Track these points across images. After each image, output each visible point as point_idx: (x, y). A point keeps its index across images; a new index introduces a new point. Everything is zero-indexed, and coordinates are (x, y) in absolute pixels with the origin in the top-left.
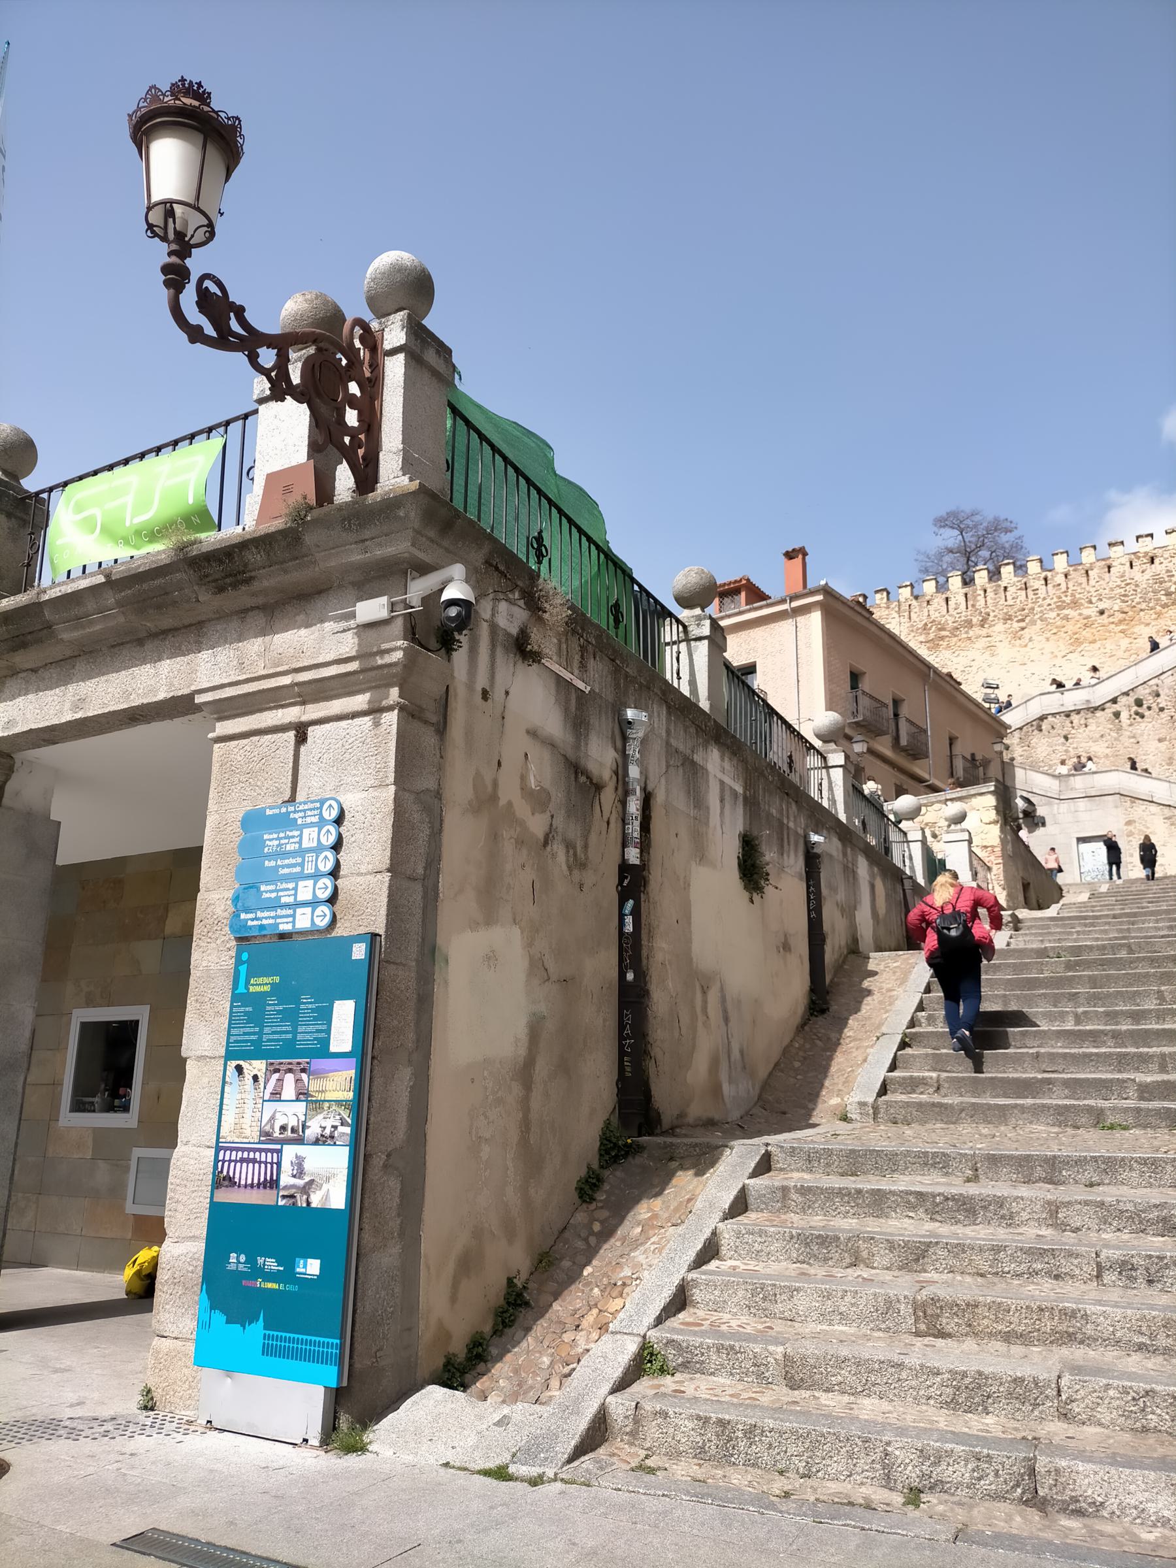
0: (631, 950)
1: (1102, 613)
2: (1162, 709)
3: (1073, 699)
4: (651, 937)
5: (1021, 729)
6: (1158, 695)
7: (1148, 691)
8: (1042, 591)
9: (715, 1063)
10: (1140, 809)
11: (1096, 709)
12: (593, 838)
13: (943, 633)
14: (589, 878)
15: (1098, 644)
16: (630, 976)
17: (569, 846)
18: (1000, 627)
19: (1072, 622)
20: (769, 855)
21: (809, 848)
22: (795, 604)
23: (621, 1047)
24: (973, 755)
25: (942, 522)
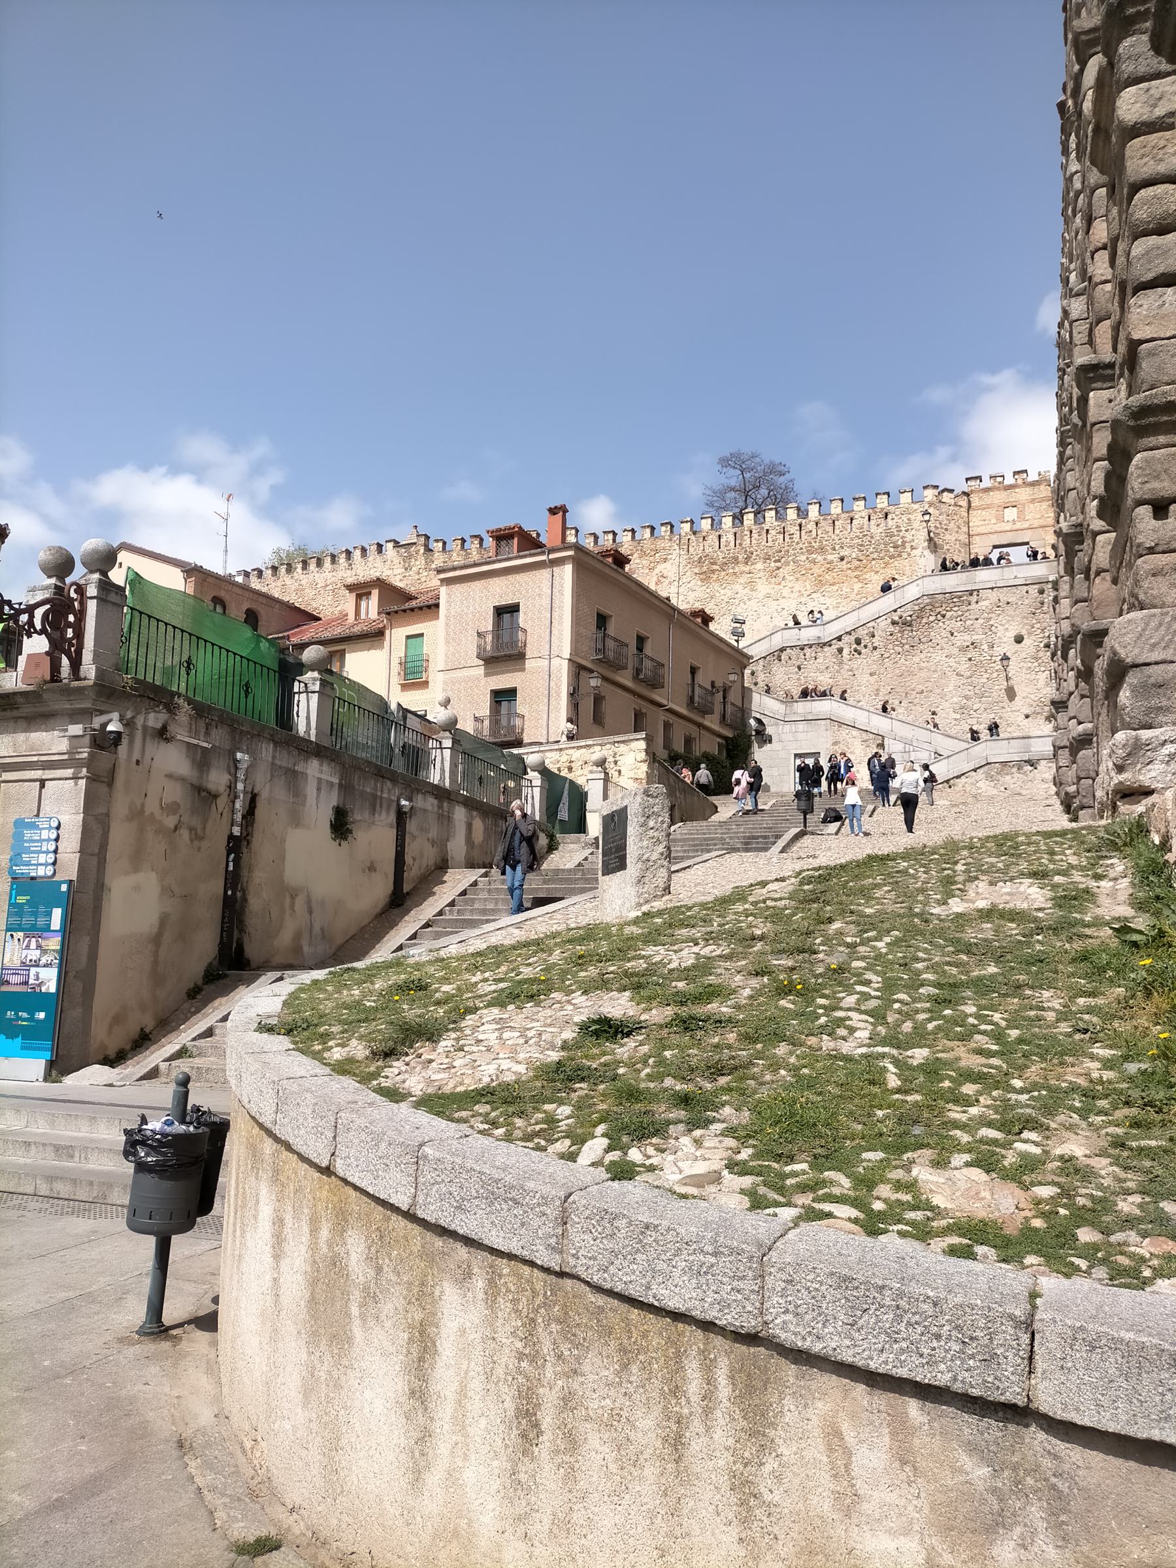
0: (233, 879)
1: (842, 559)
2: (875, 648)
3: (808, 634)
4: (250, 871)
6: (873, 636)
8: (796, 537)
9: (298, 936)
11: (825, 644)
12: (210, 824)
13: (715, 567)
14: (205, 844)
15: (835, 588)
16: (230, 893)
17: (191, 829)
18: (760, 566)
19: (818, 565)
20: (358, 815)
21: (399, 809)
22: (552, 556)
23: (222, 927)
24: (713, 683)
25: (725, 462)
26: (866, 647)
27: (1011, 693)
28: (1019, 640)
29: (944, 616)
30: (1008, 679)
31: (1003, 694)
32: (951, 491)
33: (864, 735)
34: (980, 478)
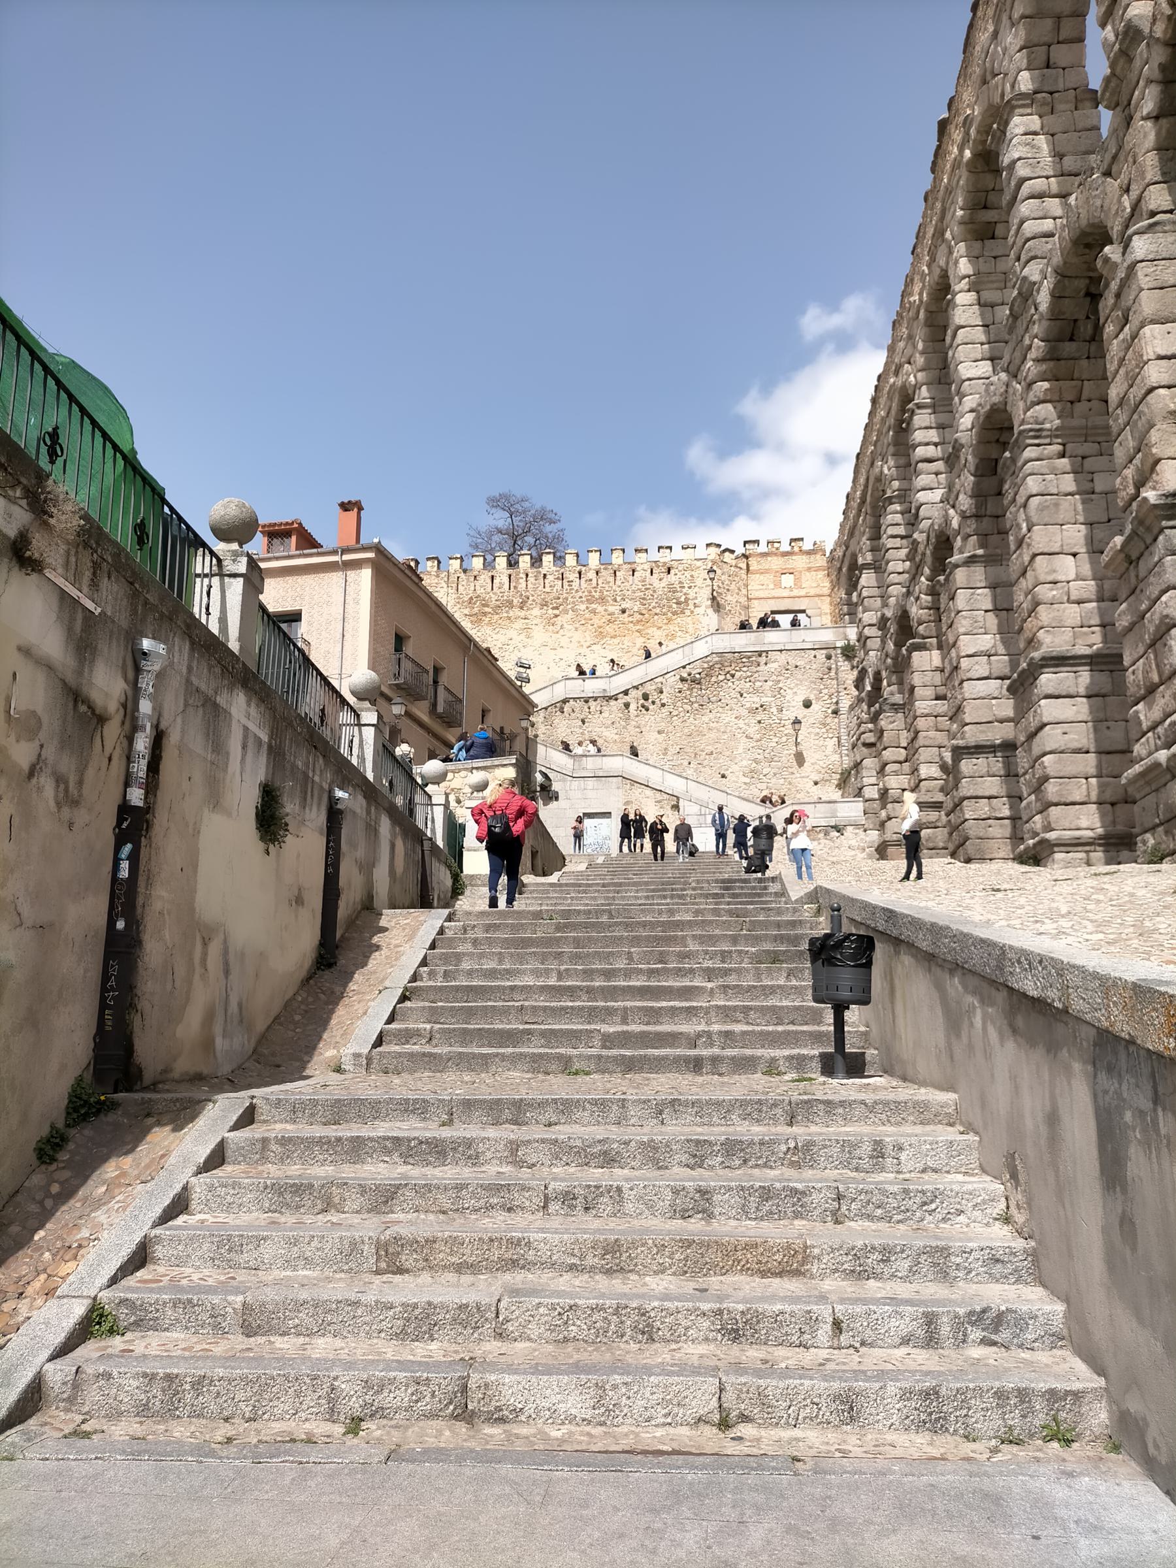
0: (125, 898)
1: (624, 611)
2: (663, 705)
3: (591, 687)
4: (149, 884)
5: (546, 708)
6: (661, 692)
7: (654, 687)
8: (576, 585)
9: (209, 1018)
10: (638, 790)
11: (610, 698)
12: (90, 773)
13: (486, 609)
14: (81, 816)
15: (616, 641)
16: (120, 925)
17: (60, 780)
18: (536, 611)
19: (599, 616)
20: (289, 807)
21: (333, 802)
22: (346, 557)
23: (103, 999)
24: (502, 728)
25: (496, 502)
26: (653, 703)
27: (800, 759)
28: (807, 704)
29: (733, 676)
30: (797, 744)
31: (792, 759)
32: (732, 552)
33: (659, 796)
34: (757, 542)
